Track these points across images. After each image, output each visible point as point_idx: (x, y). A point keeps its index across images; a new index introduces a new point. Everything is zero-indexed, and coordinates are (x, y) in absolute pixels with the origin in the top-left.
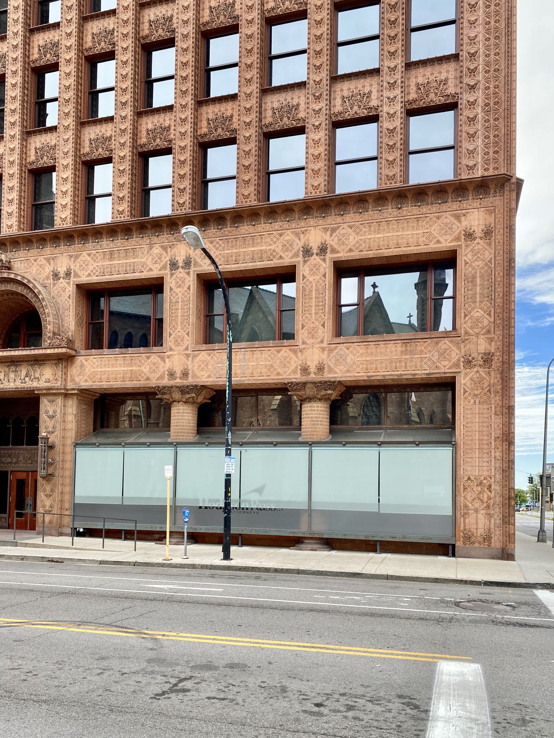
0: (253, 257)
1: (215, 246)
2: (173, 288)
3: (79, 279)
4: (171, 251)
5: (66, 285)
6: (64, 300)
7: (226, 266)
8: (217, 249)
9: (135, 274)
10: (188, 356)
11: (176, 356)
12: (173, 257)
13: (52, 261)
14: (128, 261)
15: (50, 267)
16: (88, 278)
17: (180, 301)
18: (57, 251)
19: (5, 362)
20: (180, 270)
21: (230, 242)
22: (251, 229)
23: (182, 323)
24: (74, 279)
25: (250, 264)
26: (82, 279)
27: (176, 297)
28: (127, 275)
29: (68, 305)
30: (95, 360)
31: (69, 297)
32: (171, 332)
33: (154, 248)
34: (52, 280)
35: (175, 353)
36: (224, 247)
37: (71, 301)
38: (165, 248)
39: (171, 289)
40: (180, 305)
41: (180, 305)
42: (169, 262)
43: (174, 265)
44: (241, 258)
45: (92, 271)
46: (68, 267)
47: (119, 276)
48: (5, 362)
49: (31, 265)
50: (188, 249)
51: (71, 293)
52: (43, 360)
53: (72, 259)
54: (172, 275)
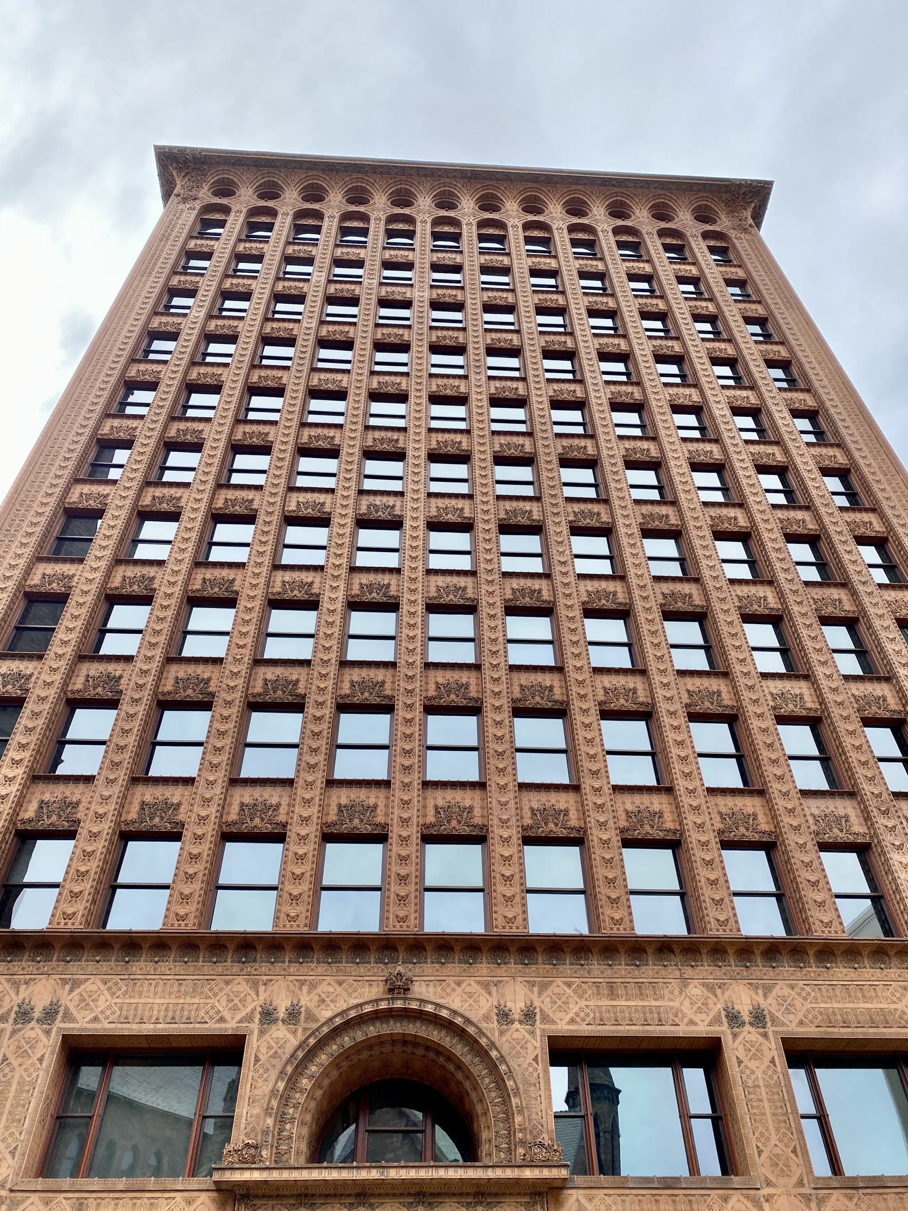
0: (871, 1018)
1: (799, 994)
2: (742, 1058)
3: (554, 1027)
4: (723, 993)
5: (527, 1035)
6: (525, 1066)
7: (830, 1030)
8: (805, 999)
9: (663, 1028)
10: (807, 1198)
11: (784, 1197)
12: (730, 1005)
13: (494, 989)
14: (646, 1003)
15: (490, 999)
16: (571, 1027)
17: (761, 1084)
18: (502, 970)
19: (401, 1194)
20: (747, 1027)
21: (824, 991)
22: (852, 974)
23: (777, 1130)
24: (542, 1026)
25: (871, 1030)
26: (559, 1027)
27: (753, 1077)
28: (647, 1028)
29: (535, 1074)
30: (609, 1200)
31: (536, 1059)
32: (759, 1145)
33: (691, 986)
34: (496, 1023)
35: (779, 1191)
36: (815, 998)
37: (540, 1067)
38: (711, 988)
39: (740, 1062)
40: (764, 1093)
41: (764, 1093)
42: (723, 1013)
43: (734, 1018)
44: (851, 1017)
45: (577, 1015)
46: (529, 1003)
47: (633, 1028)
48: (401, 1194)
49: (449, 990)
50: (753, 993)
51: (538, 1051)
52: (496, 1194)
53: (536, 989)
54: (735, 1036)
